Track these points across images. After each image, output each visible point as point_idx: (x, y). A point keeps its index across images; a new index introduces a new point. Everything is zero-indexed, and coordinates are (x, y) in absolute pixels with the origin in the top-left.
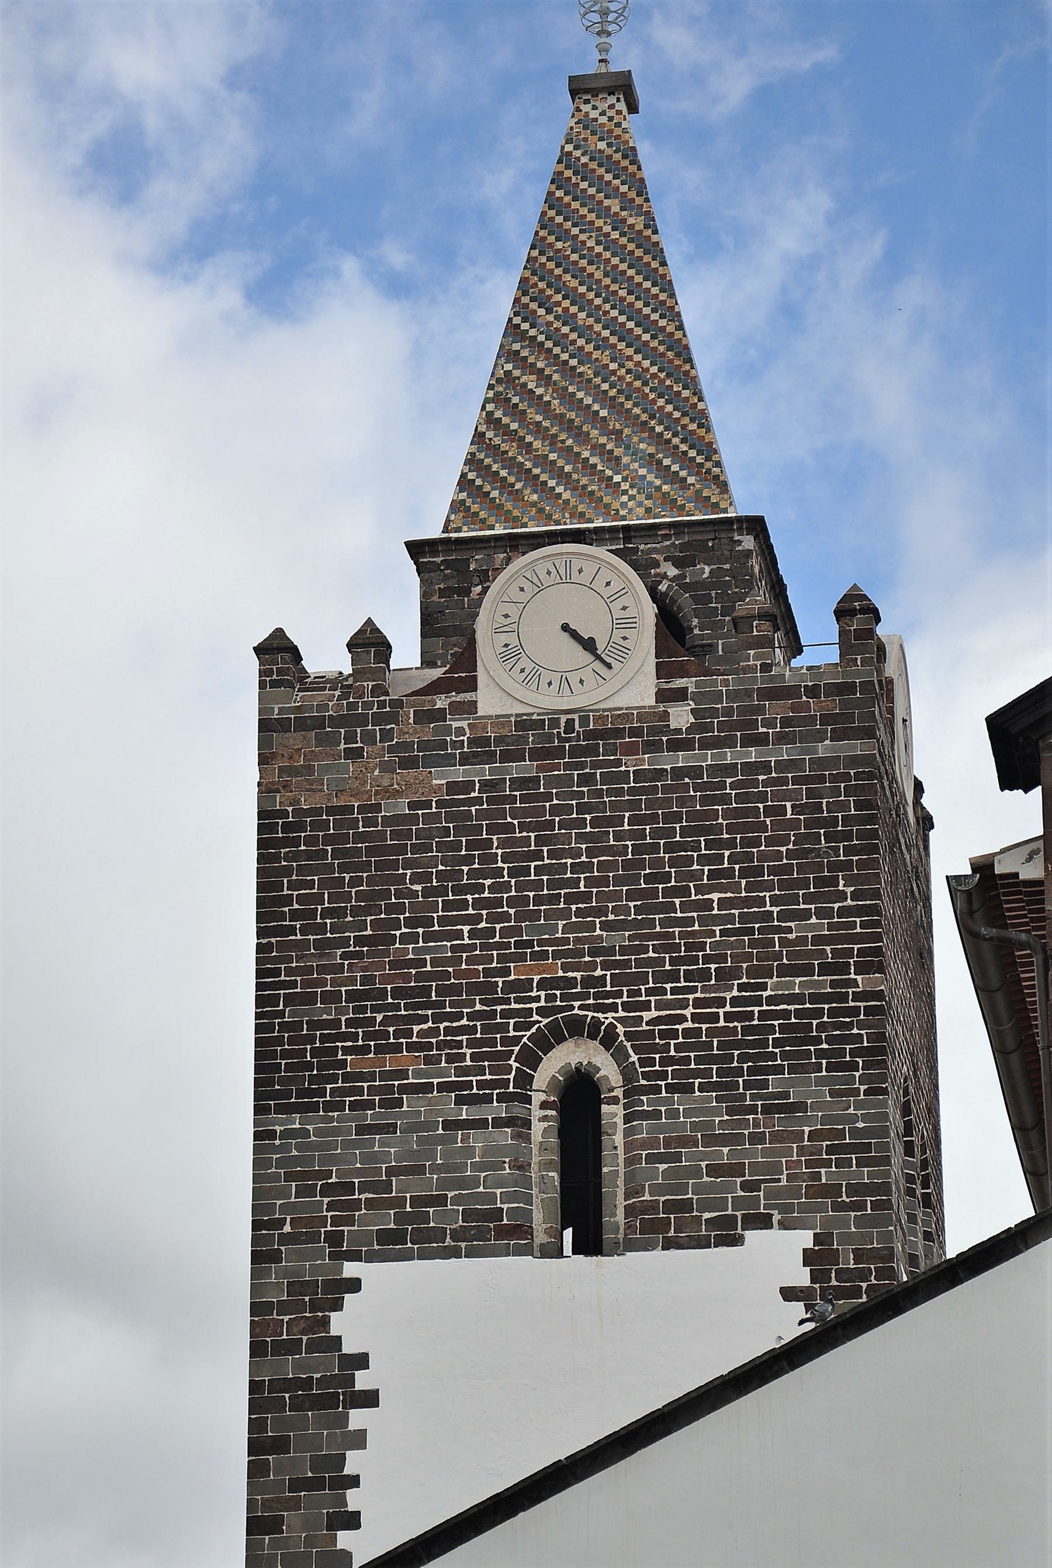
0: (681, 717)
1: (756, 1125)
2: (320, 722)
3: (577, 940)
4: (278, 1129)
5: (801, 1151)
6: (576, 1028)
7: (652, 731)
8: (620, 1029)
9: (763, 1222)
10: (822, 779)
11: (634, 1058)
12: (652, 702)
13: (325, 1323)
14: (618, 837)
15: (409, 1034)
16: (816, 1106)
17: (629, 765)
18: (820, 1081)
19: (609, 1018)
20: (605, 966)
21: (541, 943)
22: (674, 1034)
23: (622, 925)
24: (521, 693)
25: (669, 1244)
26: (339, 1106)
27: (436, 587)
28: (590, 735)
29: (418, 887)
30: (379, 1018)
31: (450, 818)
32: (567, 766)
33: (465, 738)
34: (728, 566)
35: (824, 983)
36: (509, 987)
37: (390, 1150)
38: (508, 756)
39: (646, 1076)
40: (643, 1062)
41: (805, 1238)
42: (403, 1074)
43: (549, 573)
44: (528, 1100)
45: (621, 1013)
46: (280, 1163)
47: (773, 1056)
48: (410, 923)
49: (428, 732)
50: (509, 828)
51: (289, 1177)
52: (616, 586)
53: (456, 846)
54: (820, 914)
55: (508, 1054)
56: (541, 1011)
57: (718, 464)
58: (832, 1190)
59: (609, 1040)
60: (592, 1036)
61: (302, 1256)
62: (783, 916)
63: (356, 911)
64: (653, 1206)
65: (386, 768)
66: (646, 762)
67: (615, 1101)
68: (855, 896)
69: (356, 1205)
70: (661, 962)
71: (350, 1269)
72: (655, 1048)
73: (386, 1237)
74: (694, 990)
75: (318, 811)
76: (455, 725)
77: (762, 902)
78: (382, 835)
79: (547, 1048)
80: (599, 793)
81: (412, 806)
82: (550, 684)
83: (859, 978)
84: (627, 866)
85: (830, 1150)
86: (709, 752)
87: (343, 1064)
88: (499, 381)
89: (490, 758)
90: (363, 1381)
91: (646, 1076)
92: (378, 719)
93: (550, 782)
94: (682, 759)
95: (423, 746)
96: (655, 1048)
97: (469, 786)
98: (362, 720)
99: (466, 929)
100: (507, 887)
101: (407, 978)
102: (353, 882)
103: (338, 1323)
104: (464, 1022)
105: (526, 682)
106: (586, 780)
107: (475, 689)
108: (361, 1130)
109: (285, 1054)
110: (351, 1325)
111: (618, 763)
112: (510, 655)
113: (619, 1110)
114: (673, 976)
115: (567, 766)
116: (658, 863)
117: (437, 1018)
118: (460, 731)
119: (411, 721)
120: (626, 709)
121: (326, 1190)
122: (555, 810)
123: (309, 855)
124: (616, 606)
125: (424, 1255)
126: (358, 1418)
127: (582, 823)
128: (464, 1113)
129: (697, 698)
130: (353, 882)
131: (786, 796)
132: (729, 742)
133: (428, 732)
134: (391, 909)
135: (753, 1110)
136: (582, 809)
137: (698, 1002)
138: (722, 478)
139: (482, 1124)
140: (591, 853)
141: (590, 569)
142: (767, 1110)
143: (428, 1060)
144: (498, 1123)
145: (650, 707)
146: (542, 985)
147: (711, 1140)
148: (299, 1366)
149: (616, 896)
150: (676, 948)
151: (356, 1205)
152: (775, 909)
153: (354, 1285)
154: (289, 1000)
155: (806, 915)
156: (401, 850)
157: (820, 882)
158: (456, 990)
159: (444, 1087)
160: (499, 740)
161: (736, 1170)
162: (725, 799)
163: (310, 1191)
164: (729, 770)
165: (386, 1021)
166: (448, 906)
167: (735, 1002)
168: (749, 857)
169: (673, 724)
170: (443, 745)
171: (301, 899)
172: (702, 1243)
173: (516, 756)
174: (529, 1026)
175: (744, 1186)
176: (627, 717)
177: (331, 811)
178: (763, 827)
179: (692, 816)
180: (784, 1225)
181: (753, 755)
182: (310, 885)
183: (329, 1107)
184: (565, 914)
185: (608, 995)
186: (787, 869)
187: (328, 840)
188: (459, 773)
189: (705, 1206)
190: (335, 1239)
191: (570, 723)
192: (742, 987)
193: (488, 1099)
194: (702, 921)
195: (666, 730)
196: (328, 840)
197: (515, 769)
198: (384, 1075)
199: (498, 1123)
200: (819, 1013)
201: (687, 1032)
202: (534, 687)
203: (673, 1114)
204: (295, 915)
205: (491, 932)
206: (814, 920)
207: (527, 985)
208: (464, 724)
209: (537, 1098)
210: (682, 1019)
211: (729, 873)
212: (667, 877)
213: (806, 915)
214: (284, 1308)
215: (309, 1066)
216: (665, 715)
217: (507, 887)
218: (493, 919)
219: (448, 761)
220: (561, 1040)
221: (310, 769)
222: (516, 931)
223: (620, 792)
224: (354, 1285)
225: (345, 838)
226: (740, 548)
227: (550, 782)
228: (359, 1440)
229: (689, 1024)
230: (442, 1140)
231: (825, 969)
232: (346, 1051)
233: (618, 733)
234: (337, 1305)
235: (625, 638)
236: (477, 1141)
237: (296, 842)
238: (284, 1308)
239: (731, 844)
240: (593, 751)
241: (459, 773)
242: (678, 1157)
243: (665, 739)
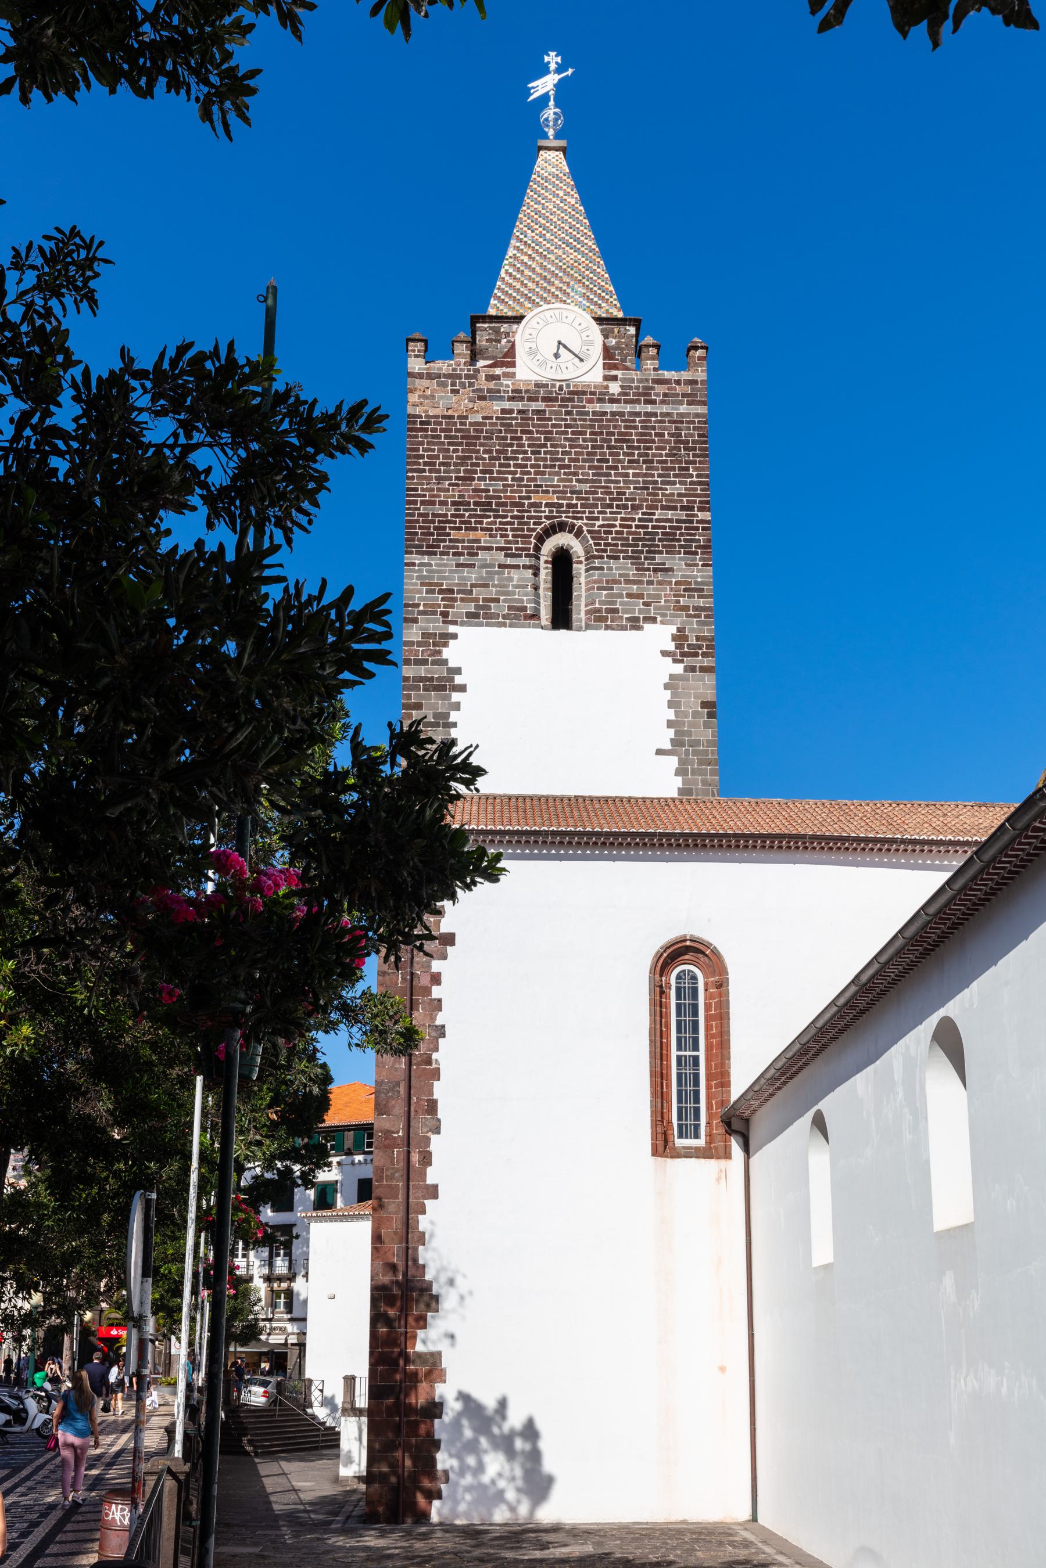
0: (615, 388)
1: (650, 576)
2: (439, 376)
3: (565, 486)
4: (417, 562)
5: (671, 589)
6: (561, 527)
7: (601, 393)
8: (585, 528)
9: (653, 620)
10: (682, 422)
11: (591, 542)
13: (440, 652)
14: (584, 440)
15: (481, 523)
16: (679, 570)
17: (590, 408)
18: (680, 559)
19: (579, 523)
20: (578, 499)
21: (546, 486)
22: (611, 533)
23: (586, 481)
24: (537, 370)
25: (607, 628)
26: (448, 554)
29: (486, 456)
30: (467, 514)
31: (502, 425)
32: (560, 406)
35: (683, 515)
36: (532, 505)
37: (472, 576)
38: (530, 399)
39: (597, 550)
40: (596, 544)
41: (673, 629)
42: (479, 541)
44: (538, 558)
45: (585, 521)
46: (418, 578)
47: (658, 546)
48: (483, 472)
49: (492, 385)
50: (531, 432)
51: (422, 584)
53: (505, 438)
54: (681, 483)
55: (530, 536)
56: (547, 517)
58: (686, 608)
59: (578, 534)
60: (570, 532)
61: (428, 621)
62: (663, 483)
63: (455, 464)
64: (599, 610)
65: (471, 400)
66: (598, 407)
67: (581, 562)
68: (698, 476)
69: (455, 600)
70: (604, 499)
71: (452, 629)
72: (601, 538)
73: (469, 615)
74: (620, 513)
75: (437, 417)
77: (653, 476)
78: (469, 431)
79: (549, 536)
80: (575, 420)
81: (484, 418)
83: (699, 514)
84: (588, 454)
85: (685, 590)
87: (449, 534)
89: (522, 399)
90: (458, 680)
91: (597, 550)
92: (467, 377)
93: (551, 413)
94: (615, 408)
95: (489, 391)
96: (601, 538)
97: (511, 411)
98: (459, 377)
99: (510, 477)
100: (529, 459)
101: (480, 497)
102: (454, 451)
103: (446, 653)
104: (509, 519)
105: (540, 365)
106: (568, 413)
108: (458, 565)
109: (420, 528)
110: (452, 654)
111: (584, 407)
112: (532, 352)
113: (583, 567)
114: (611, 506)
115: (560, 406)
116: (604, 454)
117: (495, 517)
118: (507, 386)
121: (441, 592)
122: (553, 426)
123: (433, 437)
124: (584, 335)
125: (488, 625)
126: (456, 697)
127: (567, 433)
128: (509, 561)
129: (623, 380)
130: (454, 451)
131: (665, 428)
132: (638, 402)
133: (492, 385)
134: (472, 465)
135: (648, 569)
136: (566, 426)
137: (622, 519)
139: (517, 567)
140: (571, 447)
141: (571, 316)
142: (655, 570)
143: (491, 536)
144: (525, 567)
146: (547, 505)
147: (628, 582)
148: (427, 671)
149: (583, 467)
150: (612, 493)
151: (455, 600)
152: (660, 480)
153: (454, 636)
154: (423, 503)
155: (674, 483)
156: (479, 438)
157: (681, 469)
158: (505, 504)
159: (499, 549)
160: (527, 391)
161: (640, 596)
162: (635, 427)
163: (432, 592)
164: (638, 414)
165: (470, 516)
166: (501, 465)
167: (640, 520)
168: (647, 455)
170: (499, 391)
171: (429, 457)
172: (623, 628)
173: (536, 399)
174: (540, 524)
175: (644, 604)
176: (589, 386)
177: (444, 417)
178: (654, 442)
179: (620, 434)
180: (662, 623)
181: (649, 408)
182: (434, 450)
183: (442, 553)
184: (558, 474)
185: (579, 512)
186: (665, 462)
187: (442, 430)
188: (507, 405)
189: (625, 611)
190: (445, 614)
191: (561, 388)
192: (643, 514)
193: (520, 556)
194: (625, 482)
196: (442, 430)
197: (534, 406)
198: (469, 541)
199: (525, 567)
200: (680, 528)
201: (617, 532)
203: (610, 569)
204: (425, 464)
205: (522, 479)
206: (678, 486)
207: (539, 505)
208: (509, 383)
209: (543, 559)
210: (614, 526)
211: (637, 462)
212: (607, 461)
213: (674, 483)
214: (419, 644)
215: (432, 534)
216: (607, 387)
217: (529, 459)
218: (522, 473)
219: (501, 399)
220: (555, 532)
221: (433, 397)
222: (535, 480)
223: (585, 420)
224: (454, 636)
225: (450, 430)
227: (551, 413)
228: (457, 706)
229: (618, 529)
230: (497, 573)
231: (683, 508)
232: (450, 528)
233: (584, 393)
234: (446, 645)
236: (515, 574)
237: (426, 430)
238: (419, 644)
239: (639, 448)
240: (572, 400)
241: (507, 405)
242: (612, 589)
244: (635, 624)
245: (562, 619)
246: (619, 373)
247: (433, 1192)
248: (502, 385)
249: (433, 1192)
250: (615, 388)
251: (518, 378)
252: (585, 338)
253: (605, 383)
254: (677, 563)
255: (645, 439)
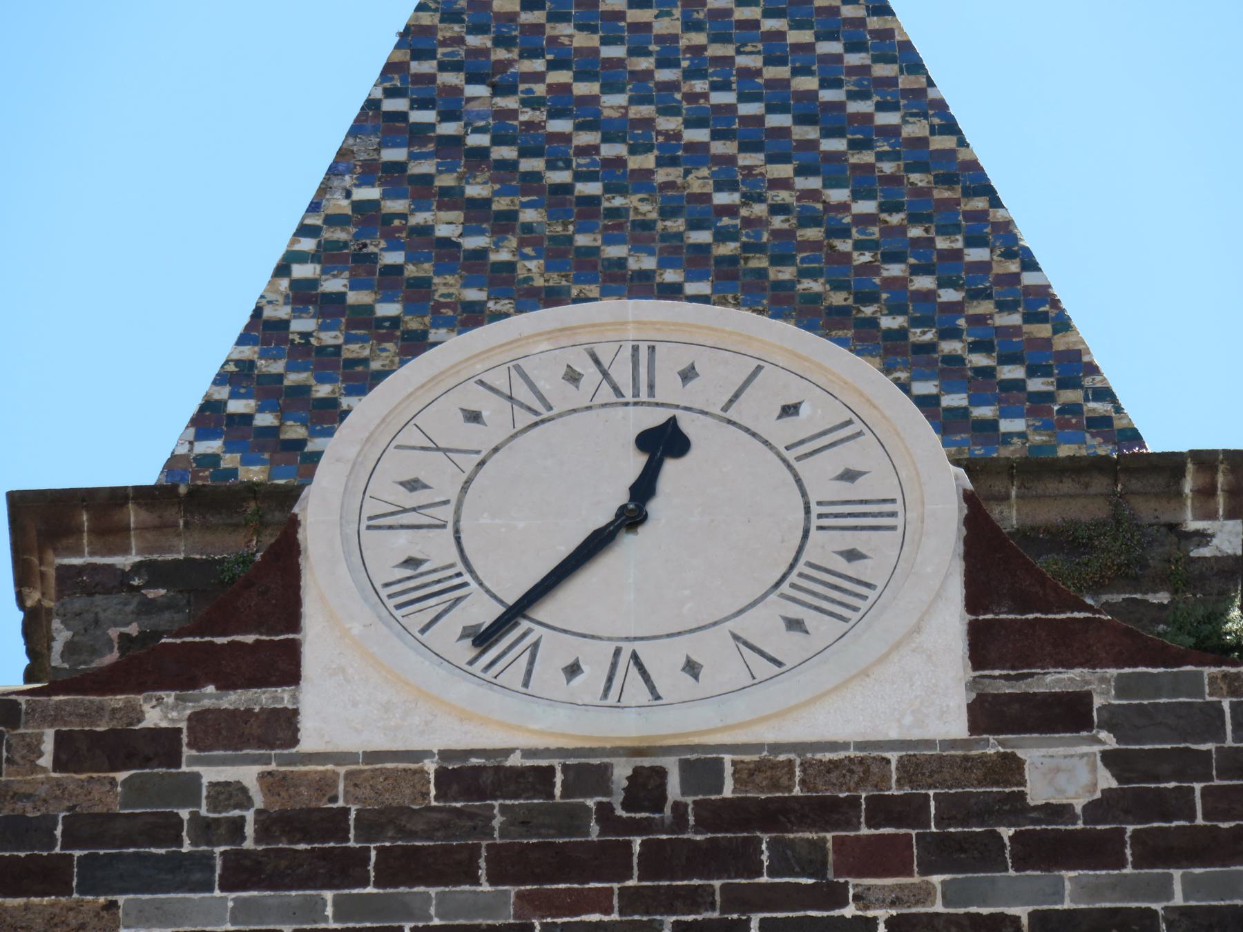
12: (958, 728)
27: (114, 633)
28: (715, 815)
33: (250, 815)
34: (1163, 598)
43: (573, 377)
52: (814, 415)
57: (1105, 394)
76: (210, 775)
82: (573, 670)
86: (1177, 874)
88: (334, 220)
95: (86, 827)
107: (292, 676)
112: (416, 592)
118: (233, 794)
119: (46, 761)
120: (860, 746)
124: (821, 476)
138: (1118, 424)
145: (953, 744)
169: (1037, 792)
195: (1015, 807)
202: (514, 676)
208: (248, 775)
216: (1011, 767)
226: (1205, 552)
235: (852, 555)
243: (1007, 832)
246: (1101, 685)
248: (189, 789)
250: (1065, 774)
251: (308, 742)
252: (823, 487)
253: (993, 746)
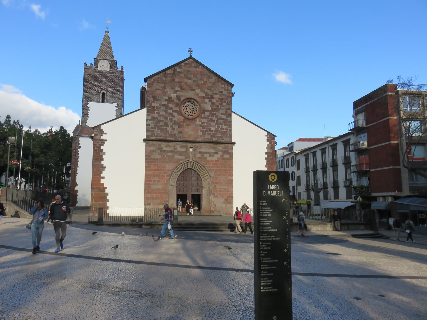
0: (111, 72)
244: (112, 103)
245: (103, 101)
247: (77, 173)
249: (77, 173)
250: (111, 72)
254: (118, 95)
255: (115, 79)
